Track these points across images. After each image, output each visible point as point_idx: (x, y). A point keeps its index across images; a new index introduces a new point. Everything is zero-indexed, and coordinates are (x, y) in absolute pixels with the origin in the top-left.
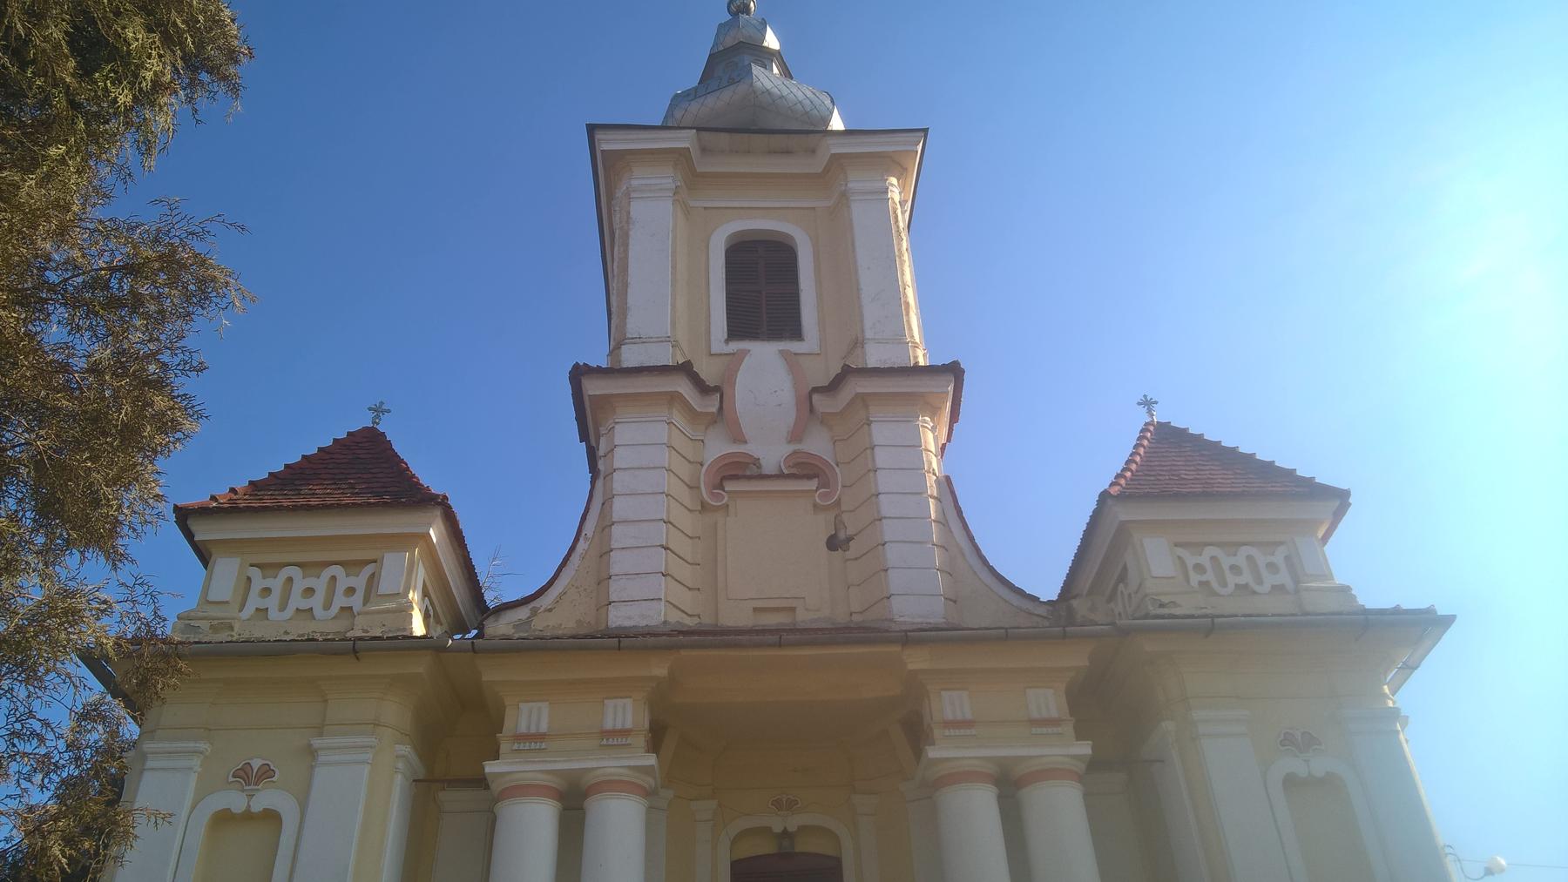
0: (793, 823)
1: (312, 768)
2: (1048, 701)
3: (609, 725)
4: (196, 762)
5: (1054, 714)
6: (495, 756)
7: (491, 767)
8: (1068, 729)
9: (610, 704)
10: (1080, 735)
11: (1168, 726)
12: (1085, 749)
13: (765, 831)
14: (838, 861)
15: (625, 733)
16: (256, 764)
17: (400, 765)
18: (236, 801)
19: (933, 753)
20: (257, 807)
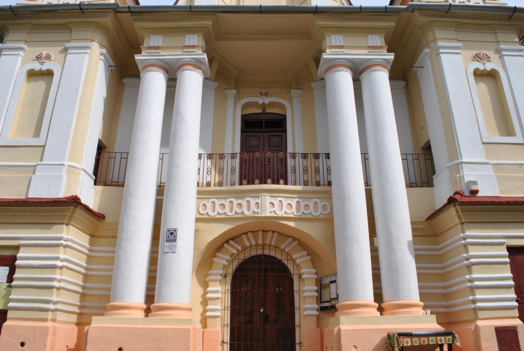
0: (267, 100)
1: (66, 55)
2: (378, 40)
3: (187, 44)
4: (21, 53)
5: (379, 44)
6: (140, 52)
7: (137, 57)
8: (385, 51)
9: (187, 36)
10: (389, 51)
11: (427, 50)
12: (391, 57)
13: (255, 104)
14: (285, 116)
15: (194, 47)
16: (44, 53)
17: (102, 58)
18: (37, 66)
19: (325, 56)
20: (44, 68)
